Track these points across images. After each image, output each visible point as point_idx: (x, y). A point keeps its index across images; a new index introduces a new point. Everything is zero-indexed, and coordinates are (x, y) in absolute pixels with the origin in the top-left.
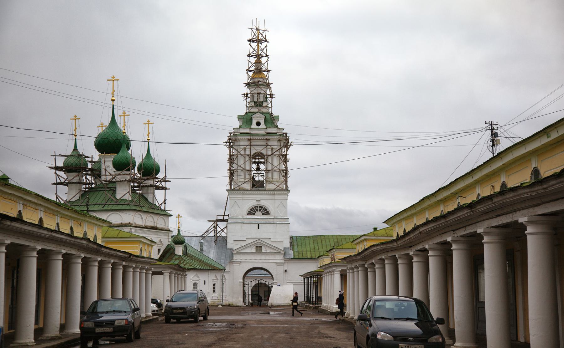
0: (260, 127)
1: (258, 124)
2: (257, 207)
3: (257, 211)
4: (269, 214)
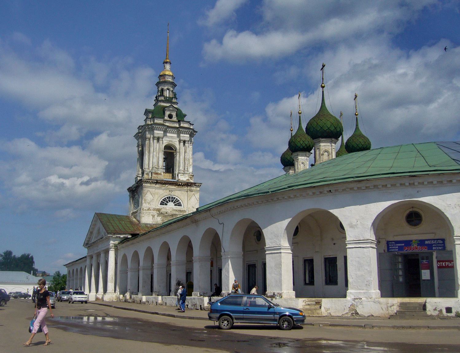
1: (170, 116)
2: (170, 197)
3: (170, 202)
4: (181, 205)
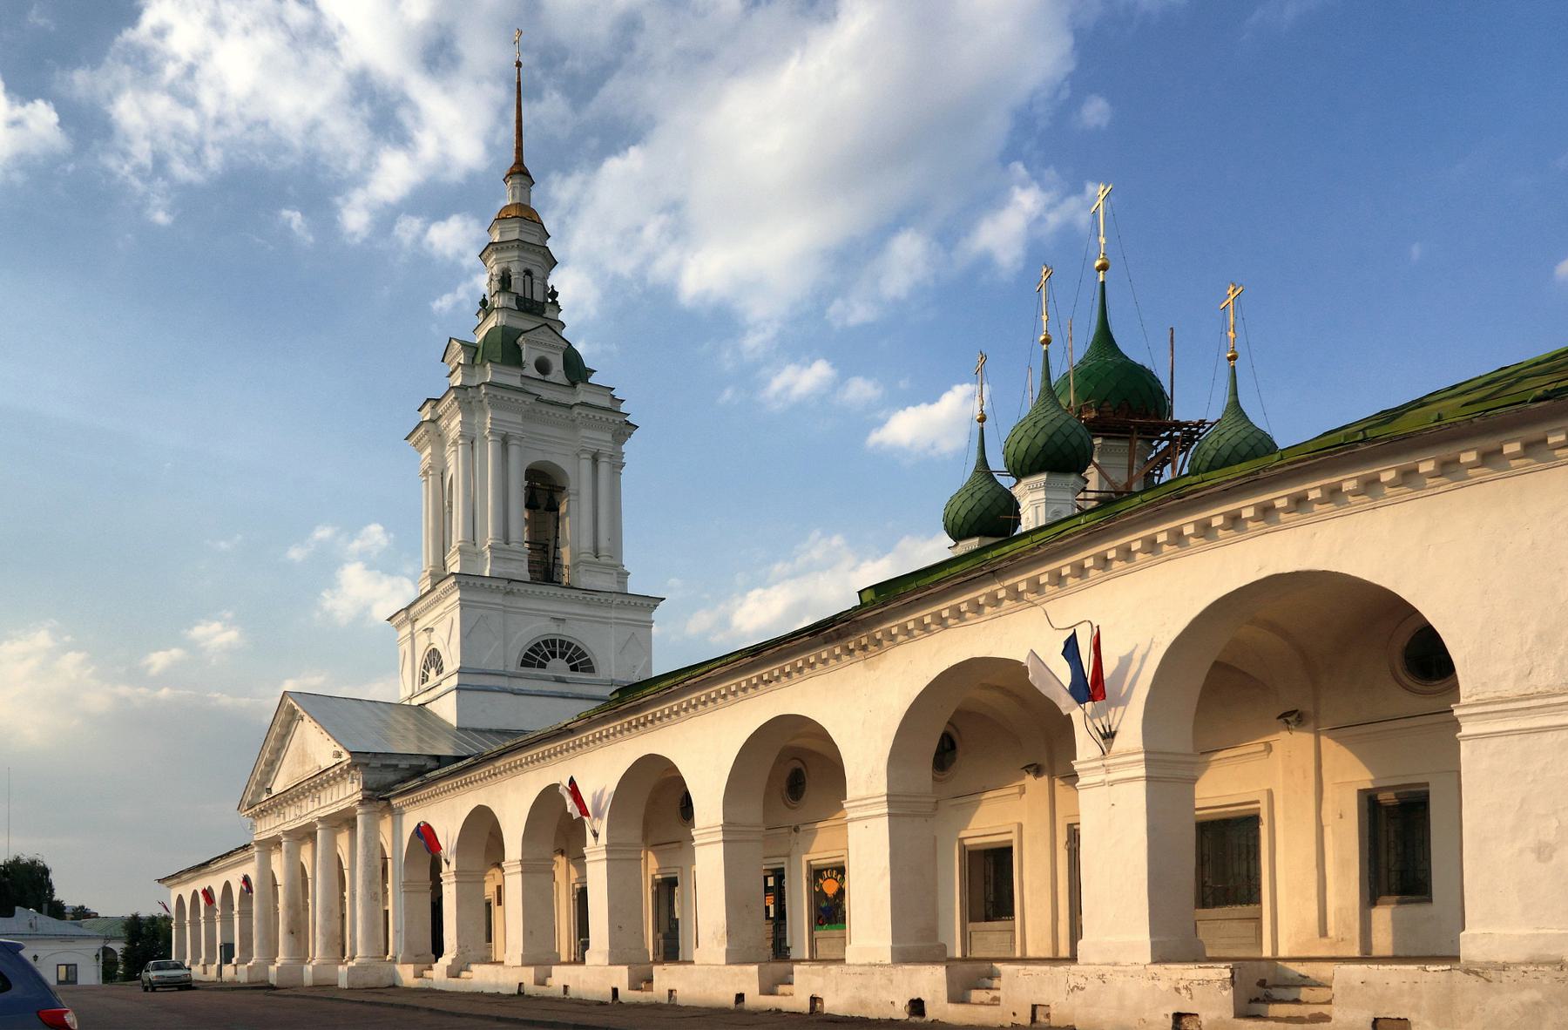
0: (548, 378)
1: (543, 366)
2: (553, 642)
4: (591, 670)
